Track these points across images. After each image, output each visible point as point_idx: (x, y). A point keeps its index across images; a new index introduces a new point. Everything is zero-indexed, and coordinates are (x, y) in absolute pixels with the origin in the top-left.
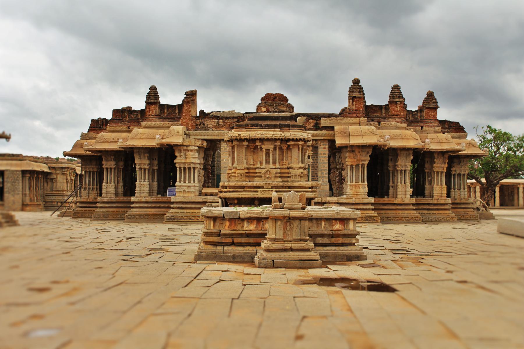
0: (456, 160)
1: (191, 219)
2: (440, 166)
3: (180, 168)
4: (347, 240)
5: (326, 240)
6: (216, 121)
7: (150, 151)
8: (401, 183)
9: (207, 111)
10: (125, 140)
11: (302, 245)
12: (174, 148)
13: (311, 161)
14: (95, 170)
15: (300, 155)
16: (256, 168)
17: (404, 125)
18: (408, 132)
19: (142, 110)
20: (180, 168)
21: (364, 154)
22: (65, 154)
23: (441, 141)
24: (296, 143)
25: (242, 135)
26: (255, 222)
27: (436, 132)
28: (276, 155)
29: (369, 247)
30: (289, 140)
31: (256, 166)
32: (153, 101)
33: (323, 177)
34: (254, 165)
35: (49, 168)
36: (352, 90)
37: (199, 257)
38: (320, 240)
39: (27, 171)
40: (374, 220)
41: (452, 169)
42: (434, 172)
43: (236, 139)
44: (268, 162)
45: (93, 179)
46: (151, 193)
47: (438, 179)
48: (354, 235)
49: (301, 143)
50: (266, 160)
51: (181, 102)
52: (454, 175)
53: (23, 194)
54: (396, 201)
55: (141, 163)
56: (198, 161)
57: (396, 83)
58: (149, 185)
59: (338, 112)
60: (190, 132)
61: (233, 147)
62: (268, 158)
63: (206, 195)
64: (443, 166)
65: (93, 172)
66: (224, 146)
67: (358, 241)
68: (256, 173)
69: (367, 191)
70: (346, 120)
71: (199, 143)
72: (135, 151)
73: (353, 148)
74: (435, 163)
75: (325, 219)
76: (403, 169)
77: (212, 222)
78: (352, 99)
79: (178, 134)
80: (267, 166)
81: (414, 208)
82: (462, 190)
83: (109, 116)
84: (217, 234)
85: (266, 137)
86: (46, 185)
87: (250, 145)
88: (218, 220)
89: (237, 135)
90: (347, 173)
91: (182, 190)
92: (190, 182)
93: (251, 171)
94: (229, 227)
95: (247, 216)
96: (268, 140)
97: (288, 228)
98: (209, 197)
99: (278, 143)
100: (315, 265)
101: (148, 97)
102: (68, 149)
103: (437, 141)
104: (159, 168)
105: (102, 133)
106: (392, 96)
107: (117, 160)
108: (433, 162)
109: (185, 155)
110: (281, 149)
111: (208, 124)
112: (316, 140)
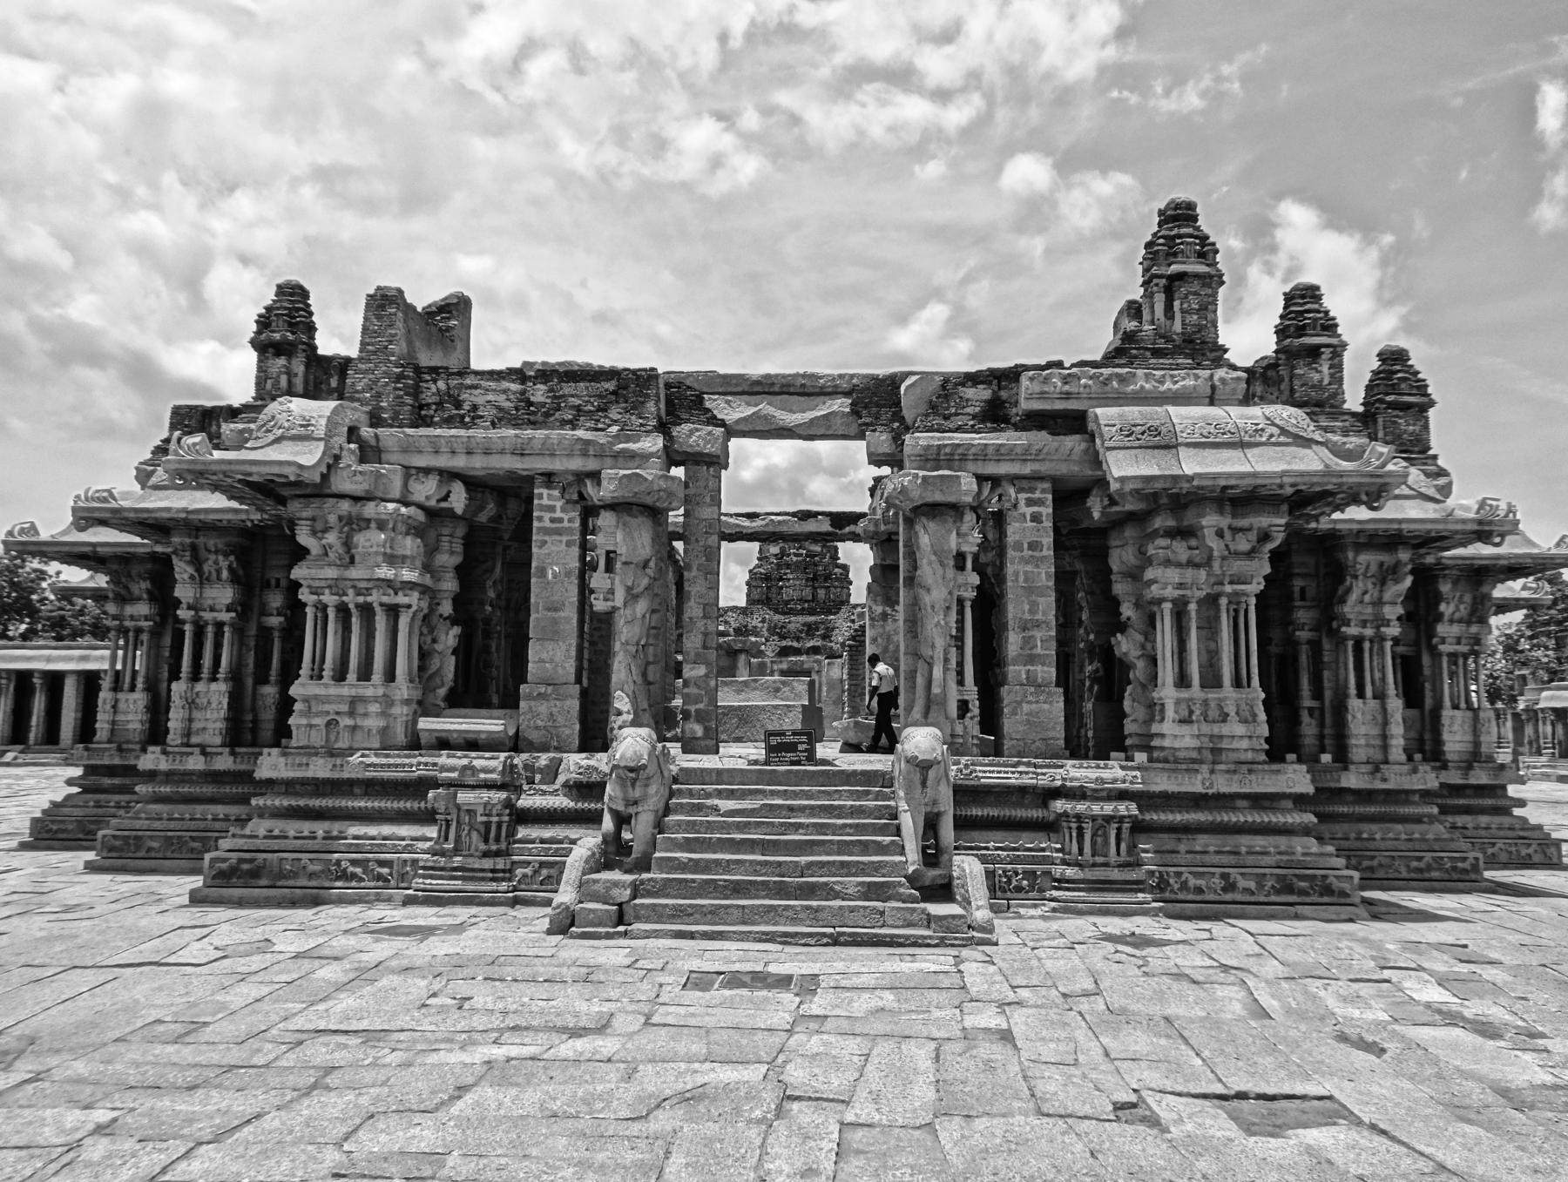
6: (515, 387)
13: (975, 579)
20: (322, 608)
33: (1032, 659)
36: (1155, 253)
40: (1328, 890)
63: (444, 743)
66: (551, 509)
71: (425, 490)
76: (1369, 632)
79: (304, 437)
91: (320, 721)
92: (365, 674)
98: (444, 759)
101: (264, 323)
109: (348, 545)
111: (480, 400)
112: (995, 481)
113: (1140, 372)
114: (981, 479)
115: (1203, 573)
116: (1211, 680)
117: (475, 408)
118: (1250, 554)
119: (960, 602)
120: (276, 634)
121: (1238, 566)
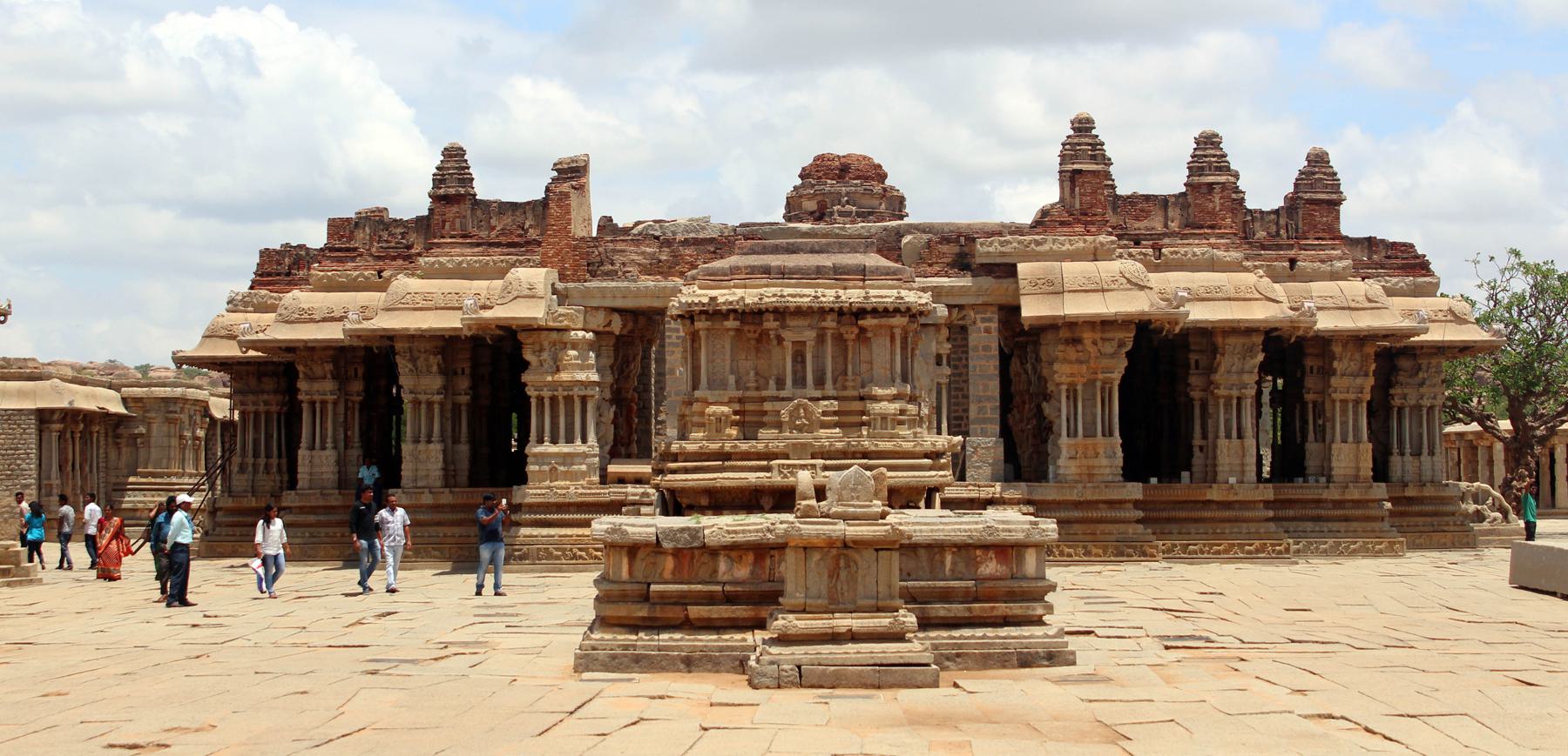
0: (1405, 363)
1: (575, 557)
2: (1350, 385)
3: (540, 399)
4: (1016, 609)
5: (957, 609)
7: (445, 343)
8: (1228, 436)
9: (621, 221)
10: (365, 312)
11: (882, 622)
12: (521, 337)
13: (947, 371)
14: (274, 408)
15: (898, 358)
16: (763, 400)
17: (1235, 255)
18: (1248, 278)
19: (419, 219)
20: (540, 399)
21: (1109, 348)
22: (180, 361)
23: (1353, 305)
24: (884, 321)
25: (721, 300)
26: (750, 557)
27: (1334, 276)
28: (824, 357)
29: (1097, 631)
30: (860, 313)
31: (765, 393)
32: (452, 191)
33: (984, 421)
34: (757, 389)
35: (125, 400)
37: (586, 662)
38: (940, 610)
39: (52, 411)
41: (1392, 391)
42: (1334, 401)
43: (702, 312)
44: (800, 381)
45: (268, 437)
46: (449, 479)
47: (1344, 423)
48: (1038, 596)
49: (899, 321)
50: (794, 373)
51: (540, 195)
52: (1400, 409)
53: (40, 488)
54: (1214, 494)
55: (418, 385)
56: (595, 377)
57: (1209, 128)
58: (444, 451)
59: (1028, 219)
60: (571, 285)
61: (694, 337)
62: (799, 367)
63: (622, 480)
64: (1359, 381)
65: (267, 413)
66: (677, 330)
67: (1050, 609)
68: (765, 413)
69: (1120, 462)
70: (1051, 242)
71: (599, 321)
72: (399, 346)
73: (1070, 330)
74: (1334, 372)
75: (955, 545)
76: (1235, 393)
77: (625, 561)
78: (1070, 179)
80: (799, 392)
81: (1271, 514)
82: (1425, 457)
83: (316, 237)
84: (641, 596)
85: (794, 302)
86: (113, 455)
87: (746, 328)
88: (641, 554)
89: (705, 300)
90: (1060, 411)
93: (750, 407)
94: (673, 573)
95: (728, 539)
96: (799, 312)
97: (843, 574)
98: (630, 489)
99: (830, 323)
100: (920, 678)
101: (438, 181)
102: (191, 345)
103: (1341, 304)
104: (475, 398)
105: (296, 293)
106: (1195, 169)
107: (340, 377)
108: (1327, 372)
109: (556, 359)
110: (839, 339)
112: (961, 307)
113: (1050, 238)
114: (950, 307)
115: (1084, 367)
116: (1090, 433)
117: (624, 264)
118: (1112, 356)
119: (939, 384)
120: (464, 408)
121: (1105, 362)
